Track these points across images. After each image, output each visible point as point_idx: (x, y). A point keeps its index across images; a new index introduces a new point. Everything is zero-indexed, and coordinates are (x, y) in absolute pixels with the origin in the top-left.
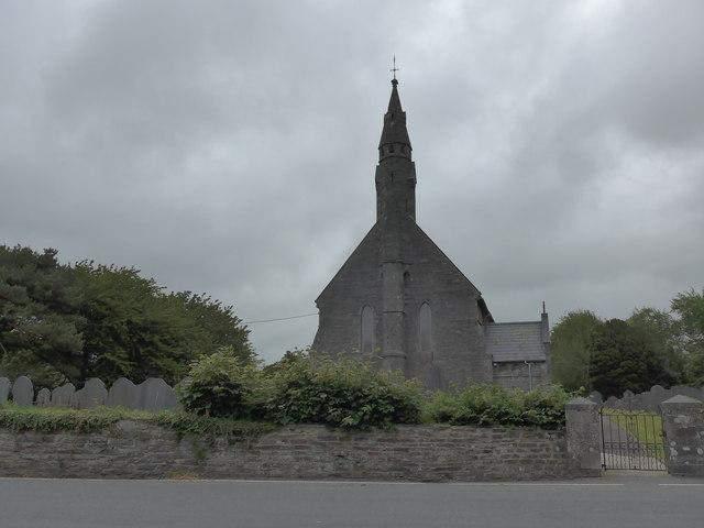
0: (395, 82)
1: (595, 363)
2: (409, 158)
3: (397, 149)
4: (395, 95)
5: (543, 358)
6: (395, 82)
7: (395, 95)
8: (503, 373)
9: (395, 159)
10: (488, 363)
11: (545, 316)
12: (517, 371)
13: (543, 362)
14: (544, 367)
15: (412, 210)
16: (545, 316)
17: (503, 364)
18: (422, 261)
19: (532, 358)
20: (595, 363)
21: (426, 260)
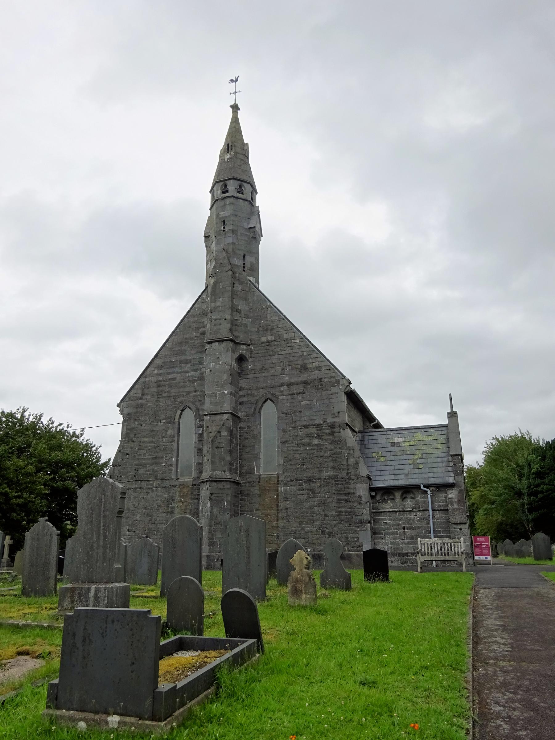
0: (235, 108)
1: (535, 494)
2: (252, 202)
3: (232, 187)
4: (235, 121)
5: (451, 480)
6: (235, 108)
7: (235, 121)
8: (388, 506)
9: (228, 201)
10: (362, 490)
11: (453, 415)
12: (409, 503)
13: (451, 486)
14: (453, 494)
15: (254, 270)
16: (453, 415)
17: (388, 491)
18: (264, 339)
19: (432, 481)
20: (535, 494)
21: (270, 338)
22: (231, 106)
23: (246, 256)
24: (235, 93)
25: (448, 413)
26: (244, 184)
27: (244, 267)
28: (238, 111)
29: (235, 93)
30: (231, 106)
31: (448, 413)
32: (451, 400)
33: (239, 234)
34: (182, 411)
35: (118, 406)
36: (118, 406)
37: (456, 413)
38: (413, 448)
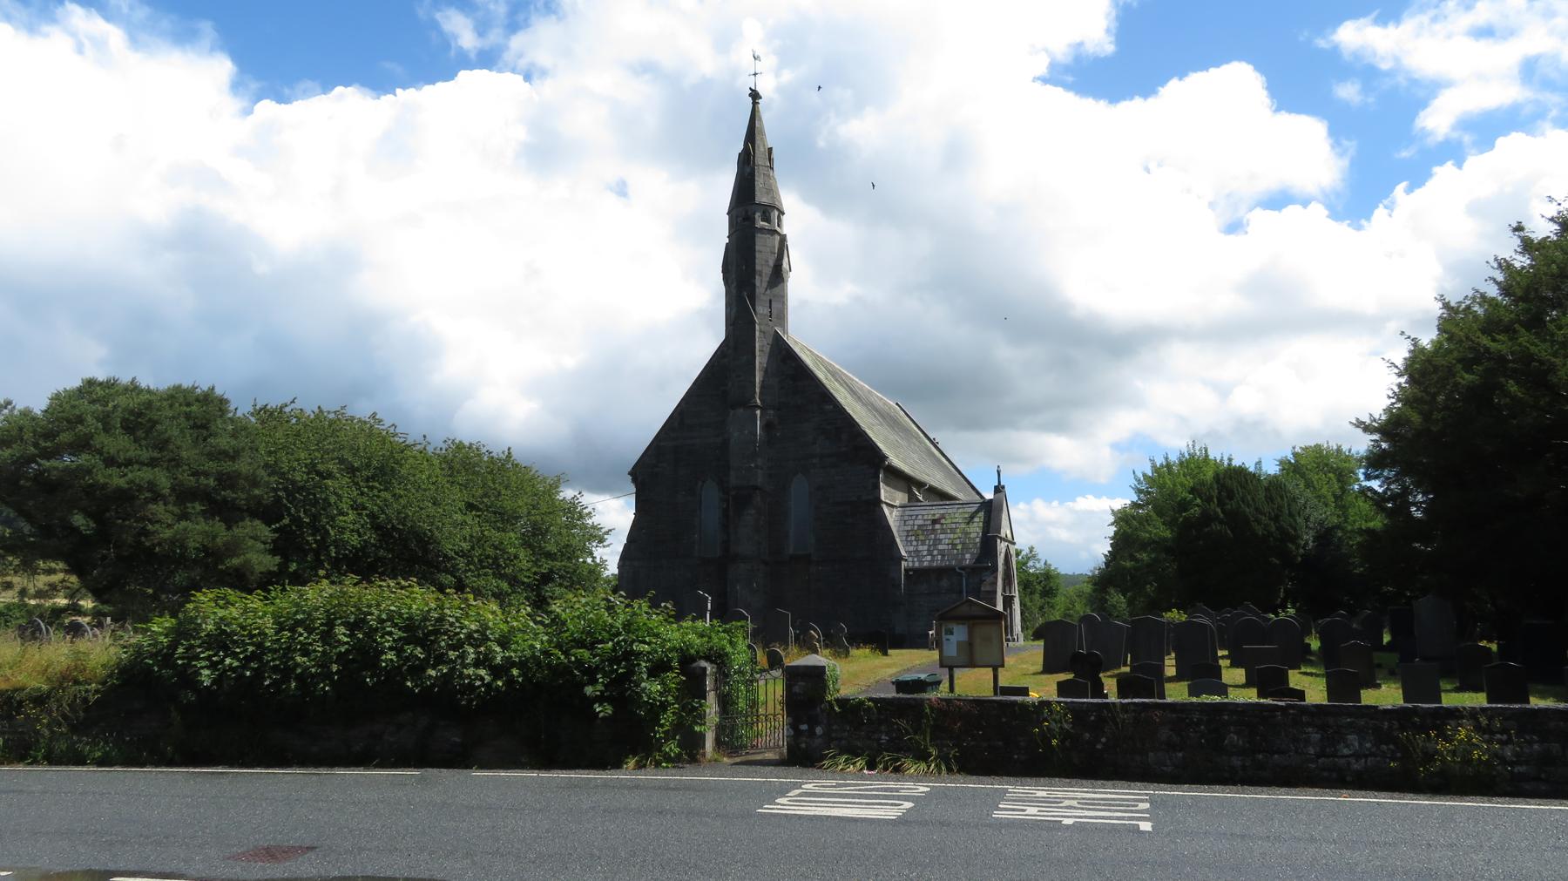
0: (755, 95)
22: (750, 95)
23: (773, 303)
24: (755, 74)
25: (995, 487)
26: (769, 208)
27: (770, 316)
28: (760, 101)
29: (755, 74)
30: (750, 95)
31: (995, 487)
32: (999, 472)
33: (764, 275)
34: (704, 482)
35: (630, 473)
36: (630, 473)
37: (1003, 487)
38: (954, 526)
